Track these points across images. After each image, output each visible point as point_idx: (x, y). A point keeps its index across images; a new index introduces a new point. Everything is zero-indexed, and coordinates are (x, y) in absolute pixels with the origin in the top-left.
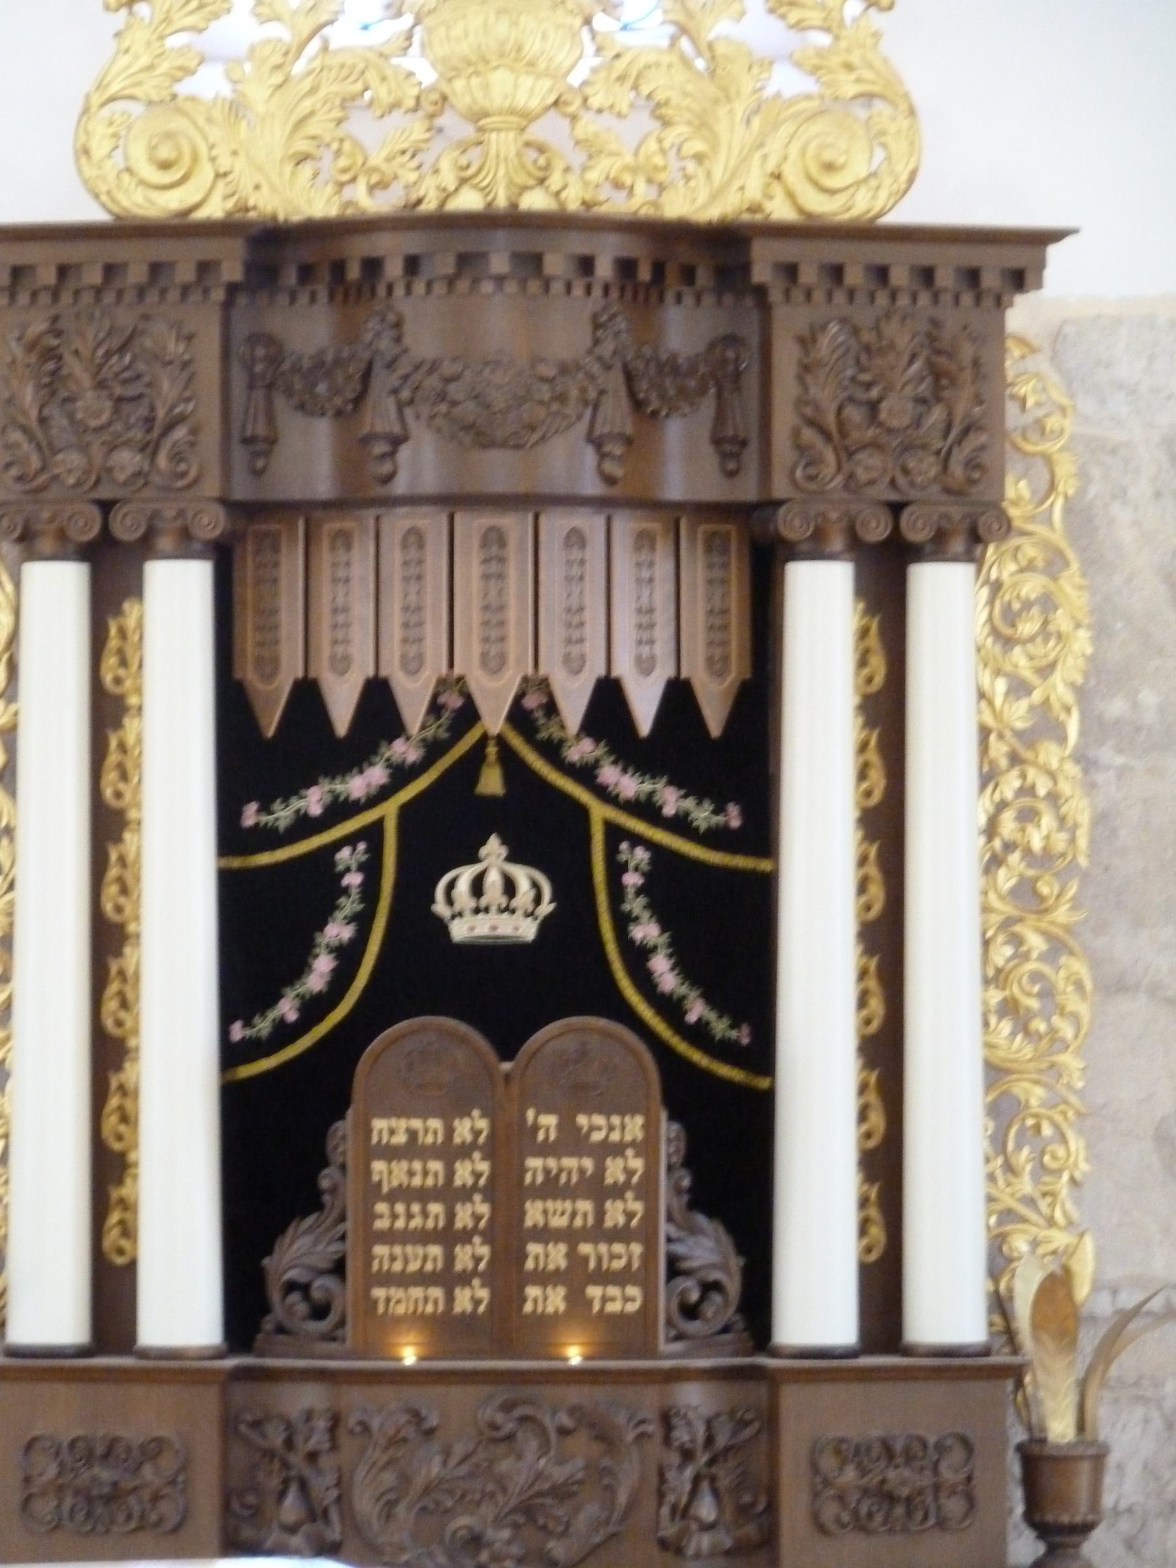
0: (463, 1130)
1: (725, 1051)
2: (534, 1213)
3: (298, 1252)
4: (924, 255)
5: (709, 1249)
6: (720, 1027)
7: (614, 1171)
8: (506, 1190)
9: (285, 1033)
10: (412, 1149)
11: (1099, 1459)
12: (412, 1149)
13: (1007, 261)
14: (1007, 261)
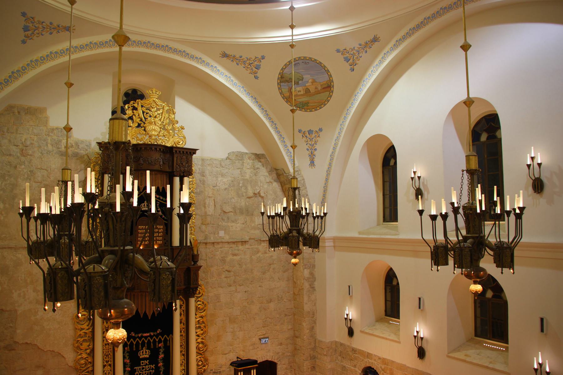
4: (187, 151)
7: (160, 231)
10: (142, 229)
11: (198, 255)
12: (142, 229)
13: (194, 151)
14: (194, 151)
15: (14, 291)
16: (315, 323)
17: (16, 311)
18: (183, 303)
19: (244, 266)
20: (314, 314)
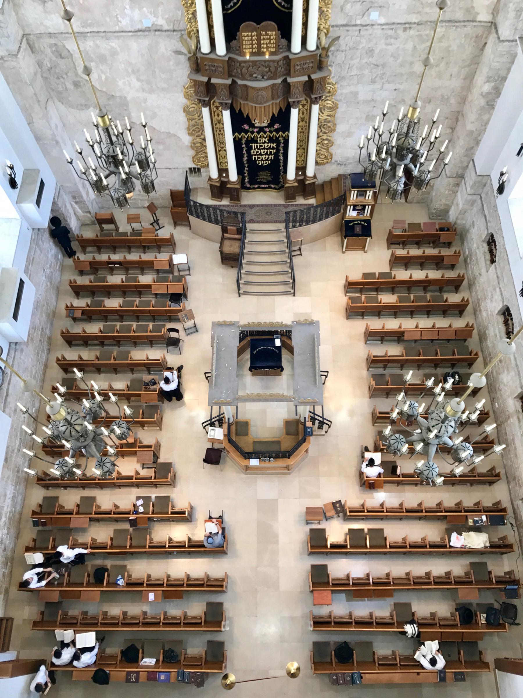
0: (253, 34)
1: (287, 8)
2: (262, 42)
3: (234, 43)
5: (284, 41)
6: (286, 5)
8: (259, 40)
9: (231, 7)
10: (247, 36)
12: (247, 36)
15: (118, 80)
16: (478, 143)
17: (125, 97)
18: (307, 102)
19: (401, 59)
20: (479, 135)
